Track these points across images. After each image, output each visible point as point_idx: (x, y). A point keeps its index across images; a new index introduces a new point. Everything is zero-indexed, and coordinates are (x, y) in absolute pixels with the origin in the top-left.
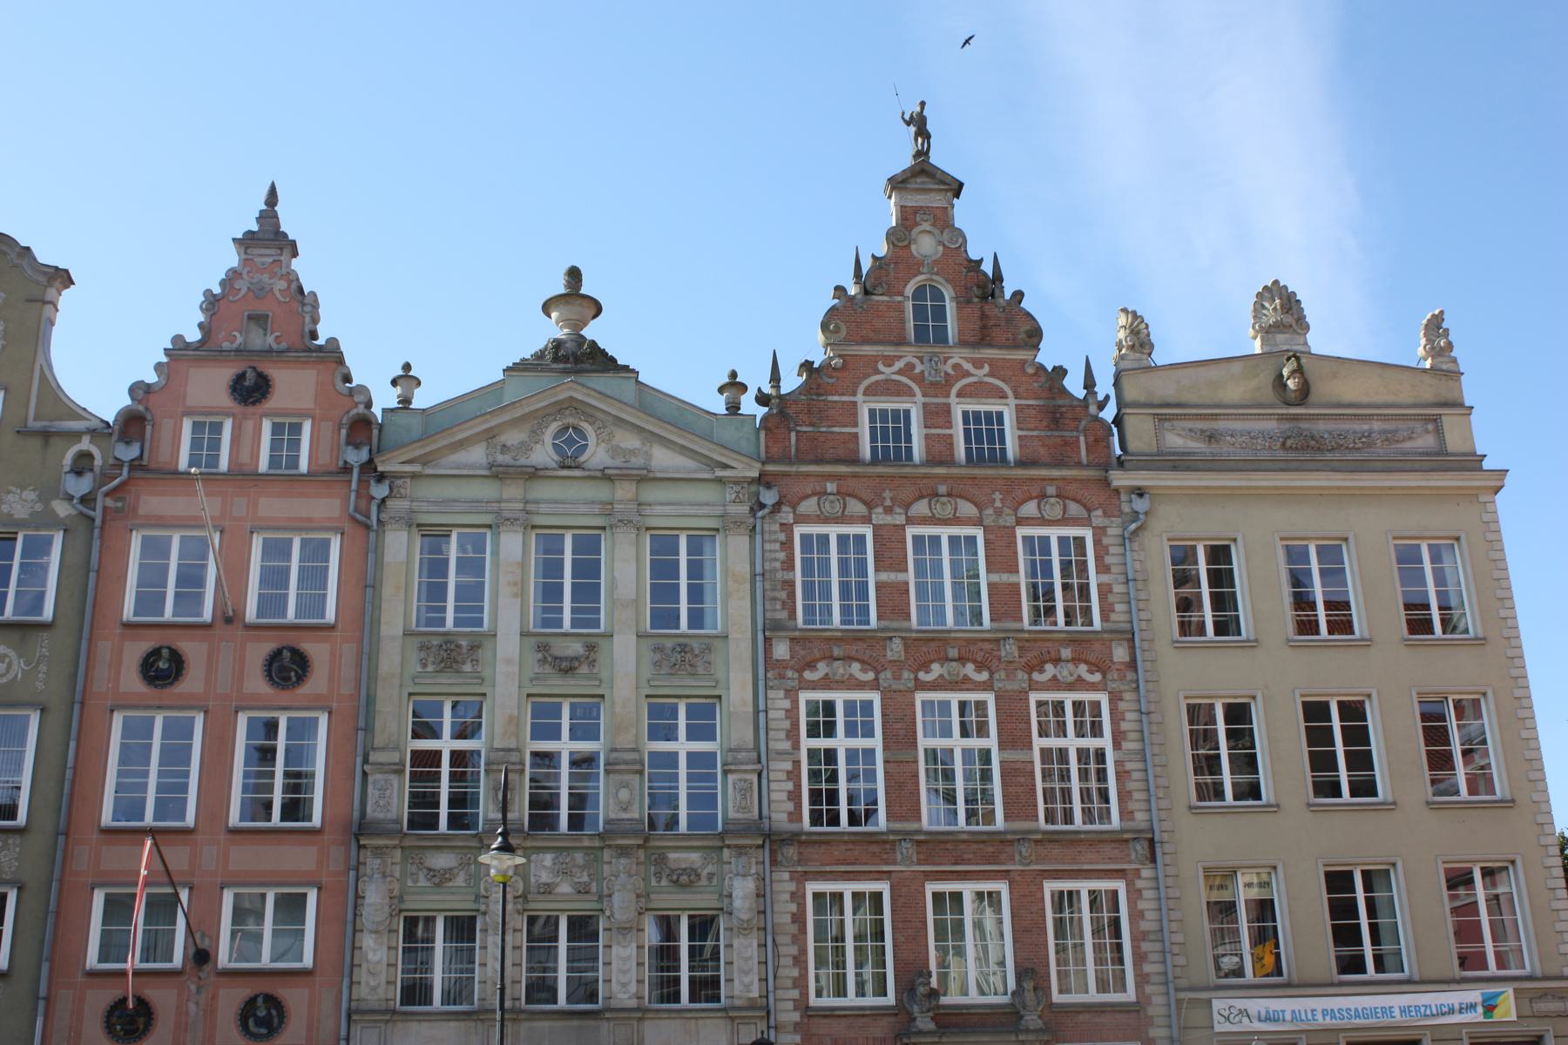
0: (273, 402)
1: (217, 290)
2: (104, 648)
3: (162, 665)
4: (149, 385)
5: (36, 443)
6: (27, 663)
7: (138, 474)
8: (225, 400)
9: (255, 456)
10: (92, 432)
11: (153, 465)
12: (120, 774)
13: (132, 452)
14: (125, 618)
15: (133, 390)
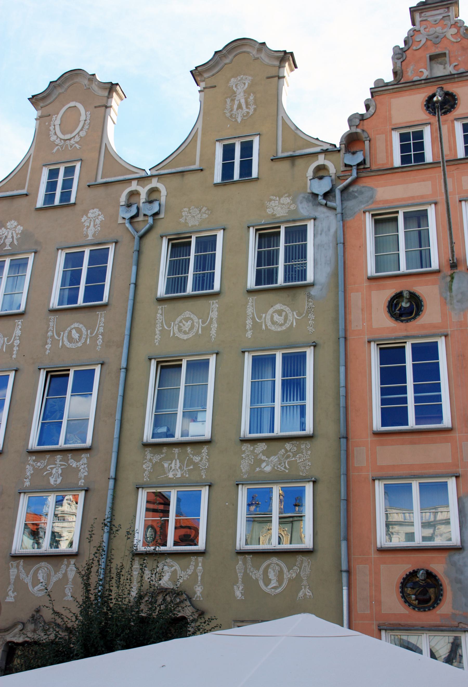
0: (459, 111)
1: (402, 45)
2: (356, 298)
3: (405, 304)
4: (362, 115)
5: (286, 165)
6: (299, 314)
7: (363, 175)
8: (423, 115)
9: (453, 148)
10: (325, 152)
11: (374, 167)
12: (384, 391)
13: (359, 158)
14: (369, 274)
15: (350, 120)
